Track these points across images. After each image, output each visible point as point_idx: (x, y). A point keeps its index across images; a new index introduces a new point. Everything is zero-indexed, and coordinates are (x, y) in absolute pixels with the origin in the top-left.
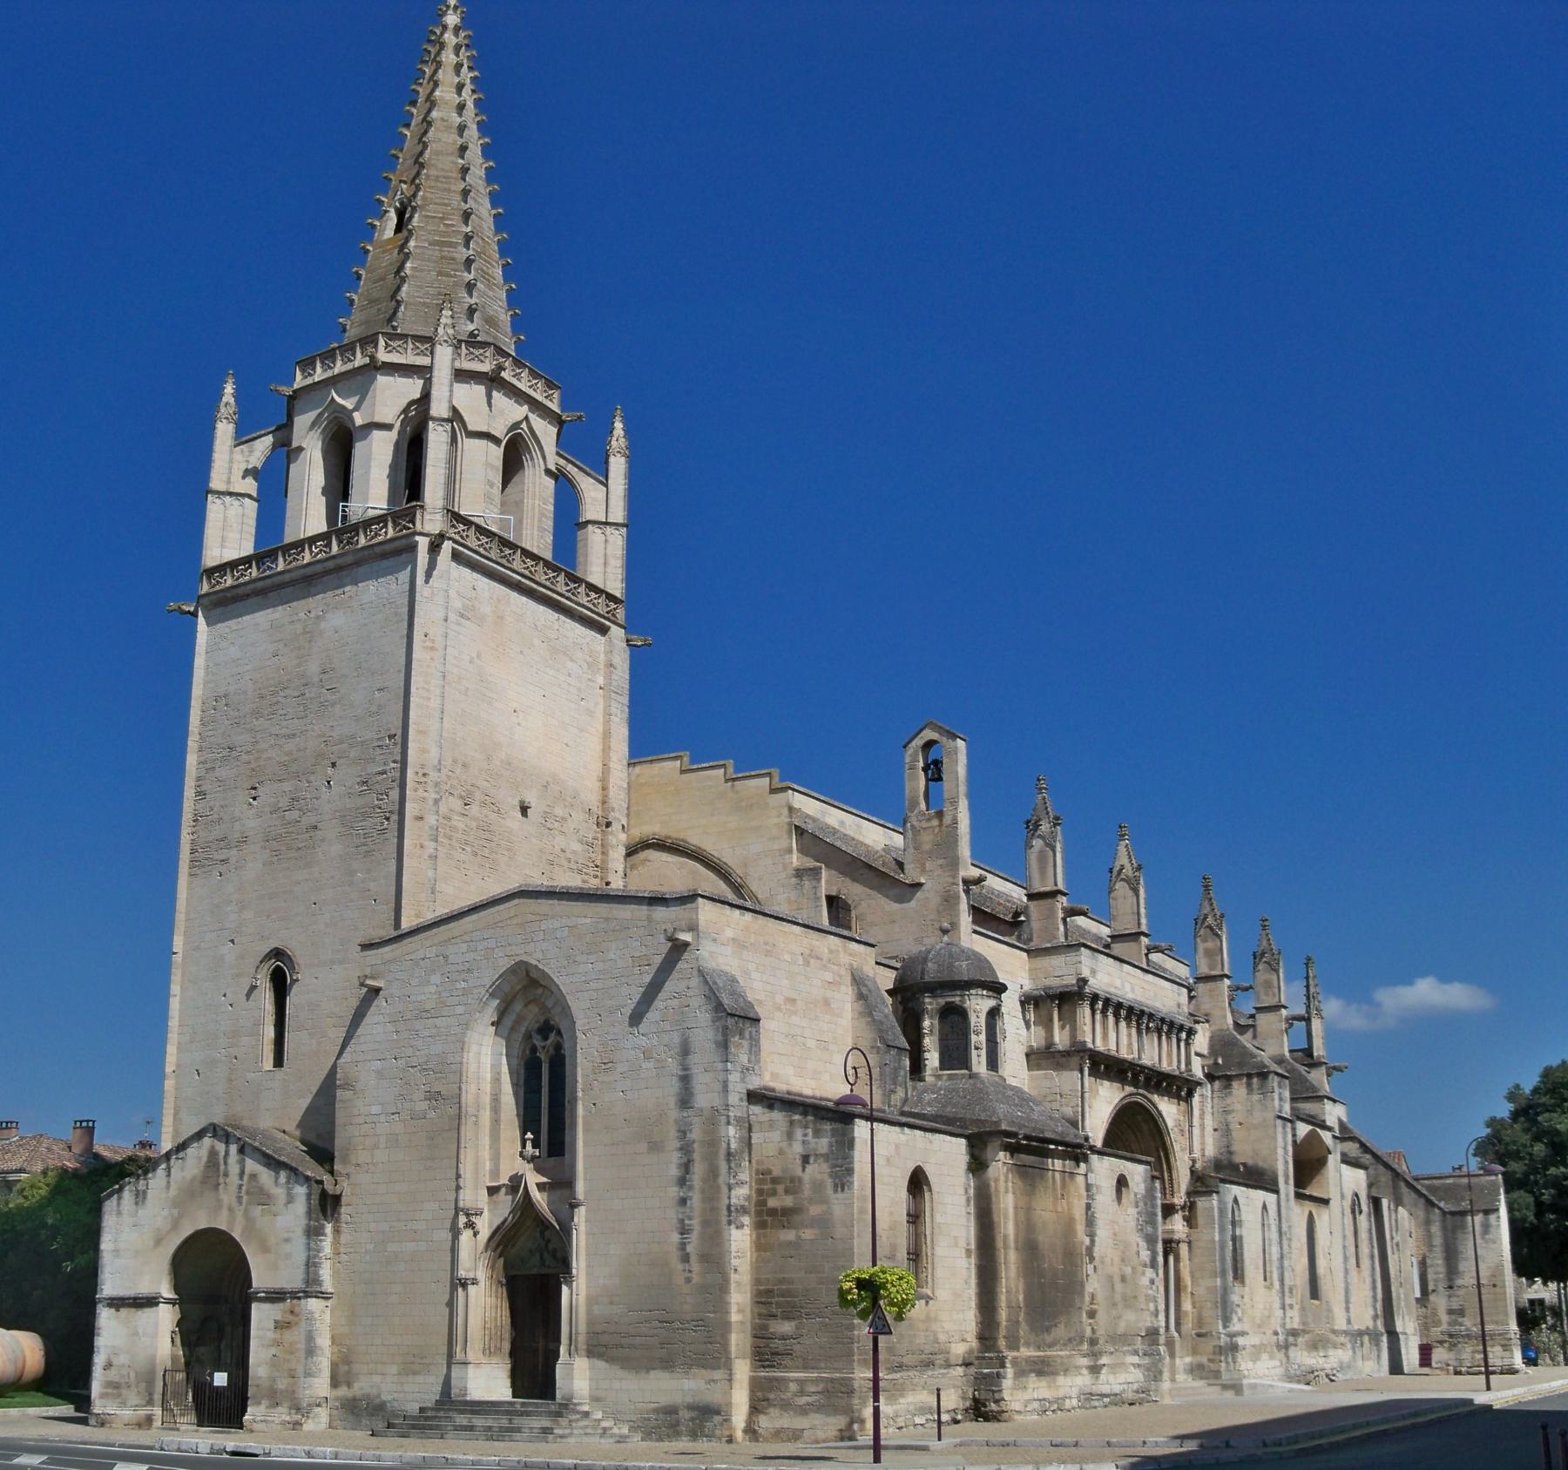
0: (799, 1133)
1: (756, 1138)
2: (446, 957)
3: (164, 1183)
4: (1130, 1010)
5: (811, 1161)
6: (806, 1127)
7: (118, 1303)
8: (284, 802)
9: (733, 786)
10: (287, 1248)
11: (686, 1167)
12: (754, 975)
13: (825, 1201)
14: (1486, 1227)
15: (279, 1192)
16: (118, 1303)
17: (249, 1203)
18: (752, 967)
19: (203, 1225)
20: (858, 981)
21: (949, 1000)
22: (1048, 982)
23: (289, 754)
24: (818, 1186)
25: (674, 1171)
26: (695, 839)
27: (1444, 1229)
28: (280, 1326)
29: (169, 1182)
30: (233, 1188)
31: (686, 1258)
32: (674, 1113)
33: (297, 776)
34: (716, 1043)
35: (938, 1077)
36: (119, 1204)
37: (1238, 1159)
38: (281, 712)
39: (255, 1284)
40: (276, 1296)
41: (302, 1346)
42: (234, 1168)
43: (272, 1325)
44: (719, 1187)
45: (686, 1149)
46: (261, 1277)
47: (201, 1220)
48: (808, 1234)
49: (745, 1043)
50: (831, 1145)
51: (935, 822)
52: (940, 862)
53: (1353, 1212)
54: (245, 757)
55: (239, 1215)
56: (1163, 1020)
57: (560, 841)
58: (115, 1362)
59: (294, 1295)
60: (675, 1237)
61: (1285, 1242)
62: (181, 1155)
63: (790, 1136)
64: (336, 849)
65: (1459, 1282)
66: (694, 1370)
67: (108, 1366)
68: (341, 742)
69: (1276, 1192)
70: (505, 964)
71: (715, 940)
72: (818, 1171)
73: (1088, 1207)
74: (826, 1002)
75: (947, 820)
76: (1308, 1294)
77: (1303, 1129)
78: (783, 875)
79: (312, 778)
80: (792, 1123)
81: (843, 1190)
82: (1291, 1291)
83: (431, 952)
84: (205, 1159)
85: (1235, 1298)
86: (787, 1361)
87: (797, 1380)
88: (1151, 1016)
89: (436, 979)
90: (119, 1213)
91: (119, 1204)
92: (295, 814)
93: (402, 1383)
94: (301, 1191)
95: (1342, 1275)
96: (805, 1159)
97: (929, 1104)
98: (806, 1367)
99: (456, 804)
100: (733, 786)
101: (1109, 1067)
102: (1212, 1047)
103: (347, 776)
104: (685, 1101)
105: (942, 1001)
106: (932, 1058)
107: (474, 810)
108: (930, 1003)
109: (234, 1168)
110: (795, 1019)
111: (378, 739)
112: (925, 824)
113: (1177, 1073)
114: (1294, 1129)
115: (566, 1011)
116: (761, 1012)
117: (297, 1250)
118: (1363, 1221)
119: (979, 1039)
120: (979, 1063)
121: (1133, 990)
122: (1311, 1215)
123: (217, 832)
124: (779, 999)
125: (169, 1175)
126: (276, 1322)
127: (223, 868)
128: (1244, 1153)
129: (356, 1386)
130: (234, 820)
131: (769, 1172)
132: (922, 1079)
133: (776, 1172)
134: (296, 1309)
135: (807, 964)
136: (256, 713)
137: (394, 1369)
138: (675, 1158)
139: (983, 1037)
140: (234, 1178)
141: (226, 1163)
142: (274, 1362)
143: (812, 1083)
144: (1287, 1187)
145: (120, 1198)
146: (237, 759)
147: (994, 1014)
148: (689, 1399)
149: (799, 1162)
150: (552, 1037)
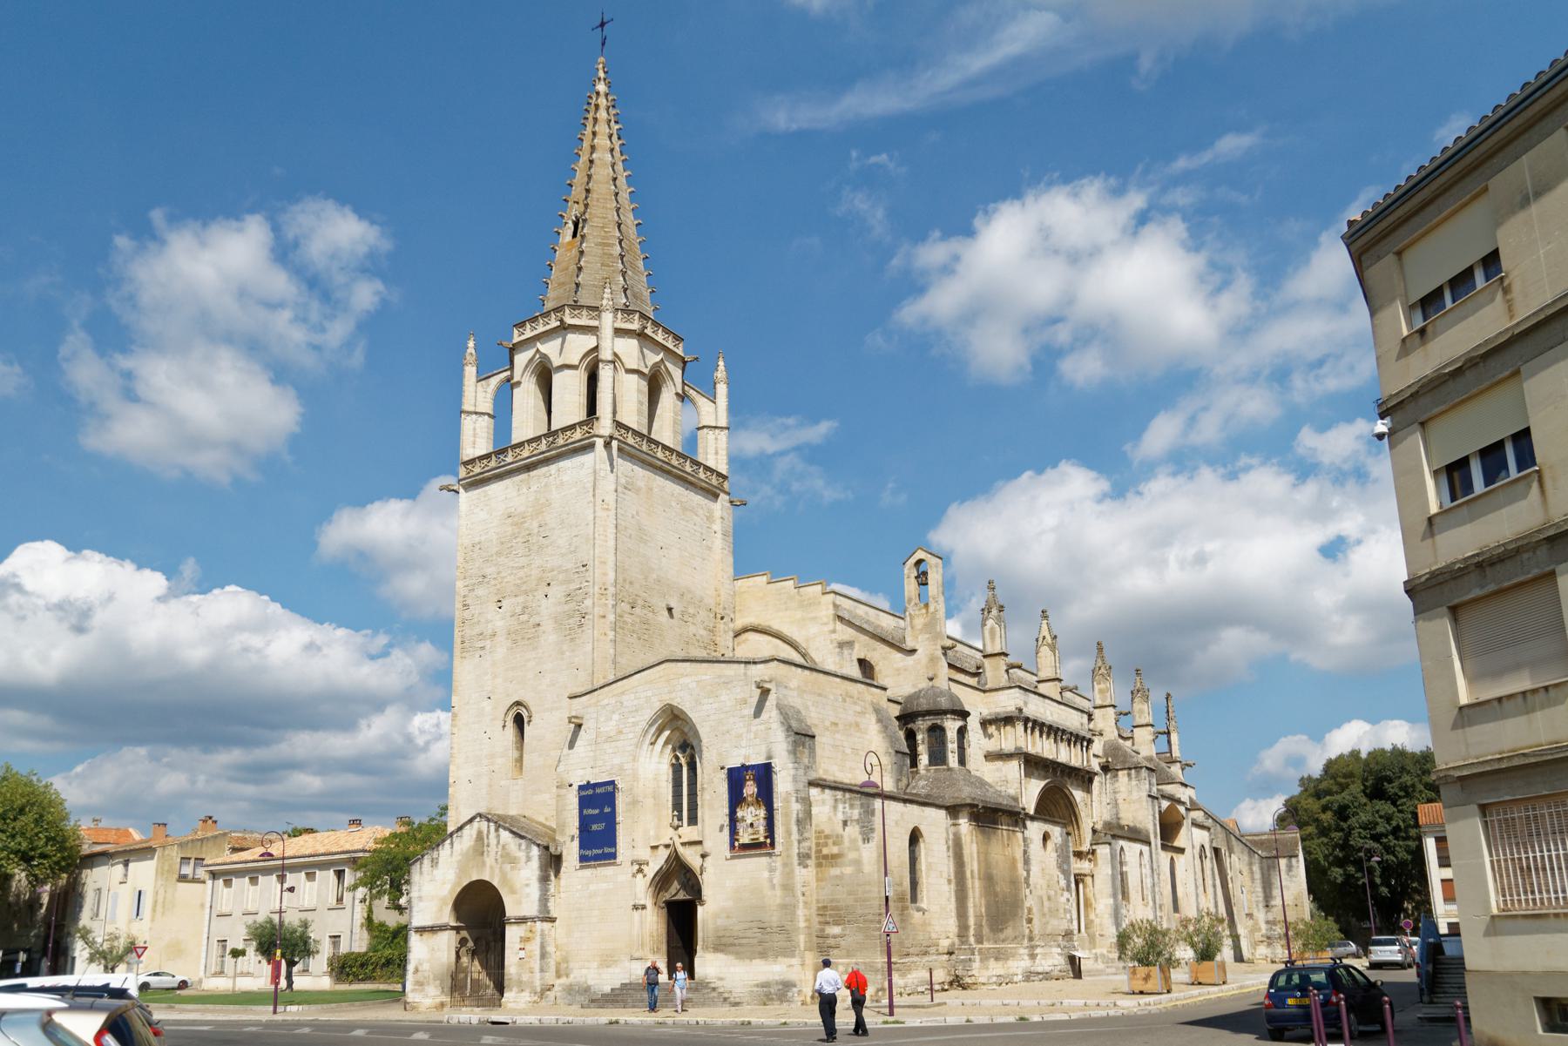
0: (840, 806)
1: (814, 810)
2: (622, 703)
3: (449, 852)
4: (1050, 727)
5: (849, 823)
6: (845, 803)
7: (422, 930)
8: (518, 610)
9: (799, 592)
10: (527, 890)
12: (812, 709)
13: (857, 849)
14: (1290, 867)
15: (522, 855)
16: (422, 930)
17: (503, 863)
18: (809, 703)
19: (474, 878)
20: (877, 711)
21: (935, 722)
22: (998, 710)
23: (521, 578)
24: (853, 841)
26: (776, 625)
27: (1262, 869)
28: (525, 940)
29: (452, 852)
30: (492, 854)
31: (773, 887)
33: (526, 593)
34: (789, 752)
35: (928, 770)
36: (421, 868)
37: (1123, 822)
38: (514, 552)
39: (507, 915)
40: (522, 920)
41: (538, 952)
42: (493, 841)
43: (519, 940)
44: (792, 841)
46: (511, 910)
48: (848, 870)
49: (806, 751)
50: (860, 814)
51: (924, 611)
52: (927, 636)
53: (1201, 857)
54: (493, 582)
55: (497, 871)
56: (1071, 733)
57: (692, 629)
58: (420, 969)
60: (766, 874)
61: (1156, 876)
62: (459, 833)
63: (835, 808)
64: (553, 638)
65: (1273, 903)
66: (780, 958)
67: (416, 971)
68: (553, 571)
69: (1149, 844)
70: (658, 706)
71: (786, 687)
72: (853, 831)
73: (1025, 852)
74: (857, 725)
75: (932, 609)
76: (1172, 909)
77: (1165, 804)
78: (831, 646)
79: (536, 594)
80: (836, 800)
81: (868, 842)
82: (1161, 906)
83: (613, 701)
84: (475, 836)
85: (1124, 911)
86: (836, 951)
87: (842, 964)
88: (1064, 731)
89: (616, 717)
90: (421, 873)
91: (421, 868)
92: (524, 618)
93: (600, 974)
94: (535, 851)
95: (1194, 898)
96: (845, 823)
97: (923, 788)
98: (848, 956)
99: (626, 607)
100: (799, 592)
101: (1034, 764)
102: (1104, 750)
103: (557, 592)
105: (930, 723)
106: (924, 759)
107: (637, 610)
108: (922, 725)
109: (493, 841)
110: (838, 736)
111: (576, 568)
112: (917, 612)
113: (1082, 767)
114: (1160, 803)
115: (696, 733)
116: (815, 731)
117: (534, 891)
118: (1208, 864)
119: (952, 746)
120: (953, 760)
121: (1052, 715)
122: (1172, 859)
123: (477, 630)
124: (827, 723)
125: (452, 848)
126: (521, 938)
127: (482, 653)
128: (1127, 818)
129: (572, 976)
130: (488, 622)
131: (823, 832)
132: (917, 772)
133: (827, 832)
134: (534, 929)
135: (844, 701)
136: (499, 554)
137: (595, 964)
139: (956, 745)
141: (488, 838)
143: (850, 776)
144: (1156, 841)
145: (421, 864)
146: (488, 583)
147: (962, 732)
148: (777, 978)
149: (841, 824)
150: (688, 751)
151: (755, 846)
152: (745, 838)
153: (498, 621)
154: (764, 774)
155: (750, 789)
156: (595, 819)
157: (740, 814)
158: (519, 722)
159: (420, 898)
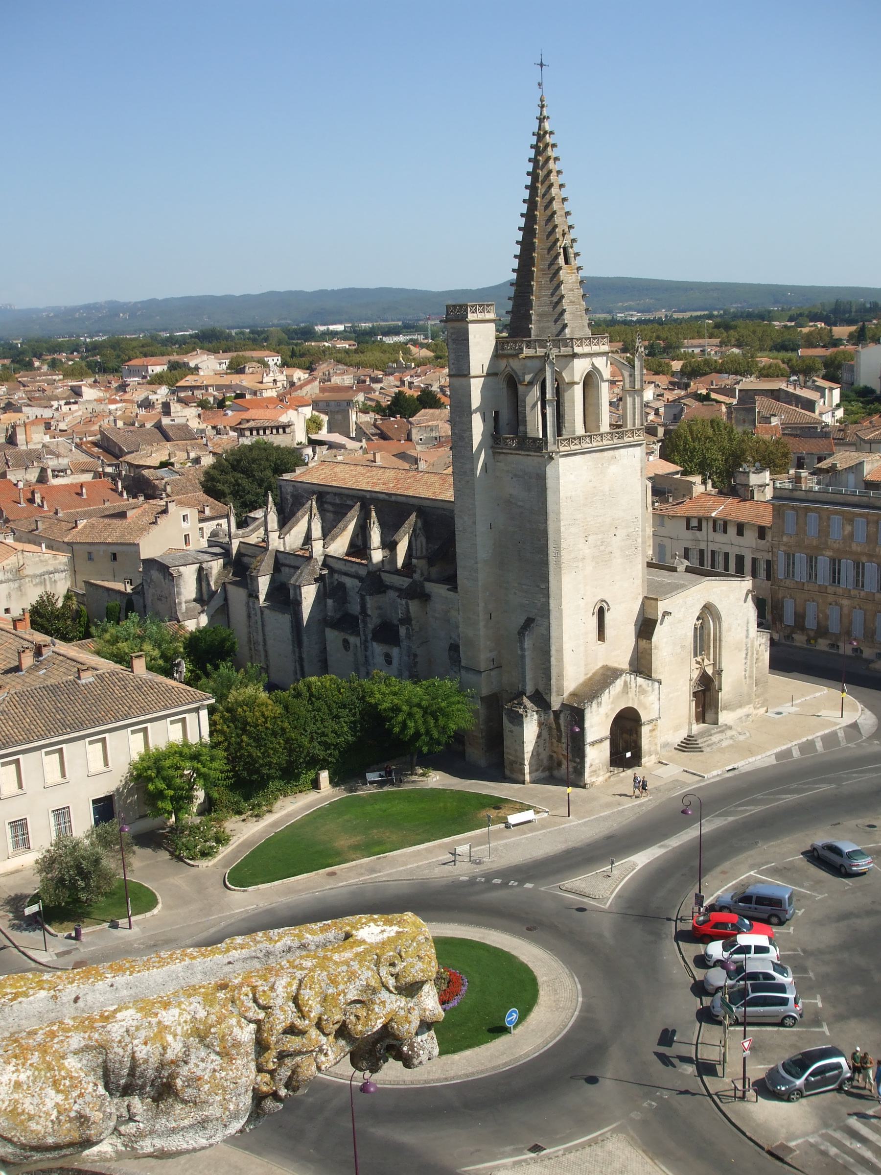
8: (599, 543)
11: (747, 654)
15: (650, 689)
16: (593, 744)
25: (744, 656)
28: (652, 731)
32: (745, 640)
42: (633, 685)
45: (747, 649)
46: (644, 719)
59: (657, 720)
67: (591, 765)
89: (683, 610)
104: (747, 637)
109: (633, 685)
138: (745, 652)
140: (633, 688)
142: (650, 743)
153: (586, 550)
158: (601, 613)
159: (592, 726)
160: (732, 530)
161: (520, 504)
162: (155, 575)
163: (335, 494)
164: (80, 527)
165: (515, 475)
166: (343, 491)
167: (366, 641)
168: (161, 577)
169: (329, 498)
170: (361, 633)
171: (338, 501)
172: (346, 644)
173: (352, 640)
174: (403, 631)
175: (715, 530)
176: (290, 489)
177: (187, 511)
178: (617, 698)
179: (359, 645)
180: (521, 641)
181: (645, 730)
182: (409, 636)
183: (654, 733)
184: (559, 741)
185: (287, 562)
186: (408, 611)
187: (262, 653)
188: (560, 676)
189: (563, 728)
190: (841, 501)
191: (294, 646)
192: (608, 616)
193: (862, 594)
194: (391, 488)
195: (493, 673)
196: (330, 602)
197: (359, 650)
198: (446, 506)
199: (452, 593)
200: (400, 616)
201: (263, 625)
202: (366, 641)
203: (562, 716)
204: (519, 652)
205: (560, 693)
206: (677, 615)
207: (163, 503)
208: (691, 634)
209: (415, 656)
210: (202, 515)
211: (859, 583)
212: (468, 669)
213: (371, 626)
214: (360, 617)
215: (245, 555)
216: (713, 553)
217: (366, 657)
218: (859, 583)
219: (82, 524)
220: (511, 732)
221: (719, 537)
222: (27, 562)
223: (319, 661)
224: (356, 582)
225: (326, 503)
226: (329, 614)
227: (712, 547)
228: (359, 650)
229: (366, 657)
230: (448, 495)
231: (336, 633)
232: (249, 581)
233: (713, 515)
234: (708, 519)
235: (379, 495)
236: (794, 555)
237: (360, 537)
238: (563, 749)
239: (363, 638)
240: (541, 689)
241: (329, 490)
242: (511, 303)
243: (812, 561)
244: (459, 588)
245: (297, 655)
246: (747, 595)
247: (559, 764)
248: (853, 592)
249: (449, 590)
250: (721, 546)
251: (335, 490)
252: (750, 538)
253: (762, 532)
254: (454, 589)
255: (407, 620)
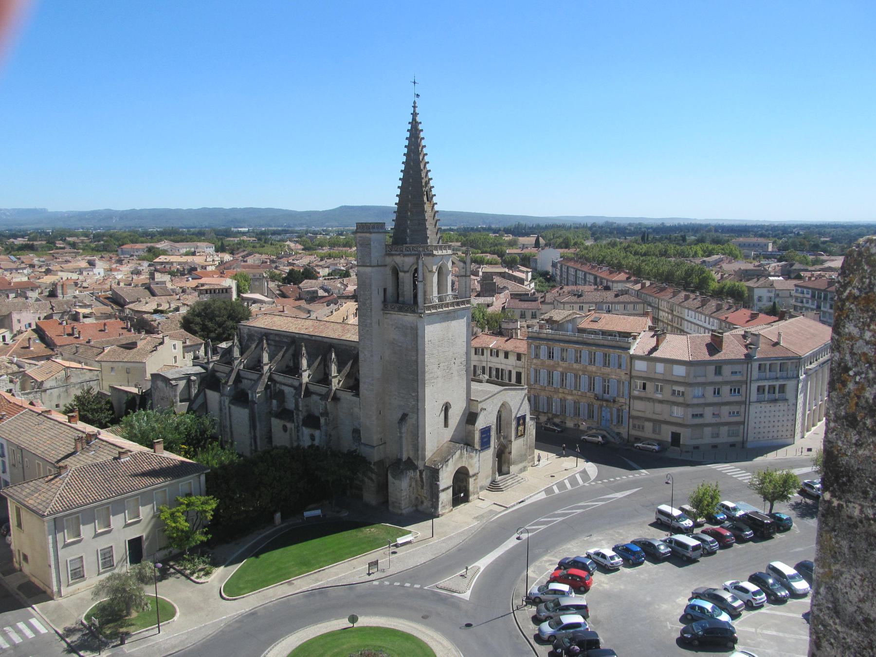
8: (446, 368)
16: (443, 490)
28: (475, 480)
46: (471, 473)
47: (460, 466)
64: (456, 378)
67: (442, 503)
127: (433, 384)
142: (474, 488)
151: (521, 435)
152: (519, 434)
153: (439, 373)
154: (524, 417)
155: (521, 422)
156: (484, 438)
157: (519, 428)
160: (502, 355)
161: (400, 344)
162: (160, 384)
163: (276, 335)
164: (106, 351)
165: (397, 327)
166: (281, 332)
167: (298, 426)
168: (164, 385)
169: (272, 337)
170: (295, 421)
171: (277, 339)
172: (285, 429)
173: (289, 425)
174: (322, 420)
175: (491, 355)
176: (246, 331)
177: (176, 342)
178: (457, 461)
179: (293, 428)
180: (400, 428)
181: (471, 480)
182: (327, 424)
183: (477, 481)
184: (422, 487)
185: (246, 376)
186: (326, 408)
187: (229, 434)
188: (424, 449)
189: (424, 480)
190: (568, 340)
191: (250, 430)
192: (450, 412)
193: (579, 393)
194: (311, 331)
195: (381, 447)
196: (274, 402)
197: (293, 431)
198: (353, 344)
199: (355, 398)
200: (321, 411)
201: (230, 416)
202: (298, 426)
203: (424, 473)
204: (399, 435)
205: (424, 458)
206: (489, 409)
207: (160, 336)
208: (495, 421)
209: (330, 435)
210: (185, 345)
211: (577, 387)
212: (366, 445)
213: (301, 417)
214: (295, 411)
215: (217, 371)
216: (490, 368)
217: (298, 436)
218: (577, 387)
219: (107, 350)
220: (394, 483)
221: (494, 359)
222: (73, 375)
223: (266, 438)
224: (292, 389)
225: (270, 340)
226: (274, 409)
227: (489, 365)
228: (293, 431)
229: (298, 436)
230: (355, 338)
231: (278, 421)
232: (221, 388)
233: (491, 346)
234: (487, 348)
235: (304, 336)
236: (539, 371)
237: (292, 361)
238: (425, 492)
239: (296, 424)
240: (411, 457)
241: (272, 332)
242: (394, 223)
243: (550, 375)
244: (361, 396)
245: (253, 434)
246: (525, 396)
247: (422, 502)
248: (574, 392)
249: (353, 396)
250: (494, 364)
251: (275, 332)
252: (512, 359)
253: (519, 357)
254: (357, 395)
255: (326, 414)
